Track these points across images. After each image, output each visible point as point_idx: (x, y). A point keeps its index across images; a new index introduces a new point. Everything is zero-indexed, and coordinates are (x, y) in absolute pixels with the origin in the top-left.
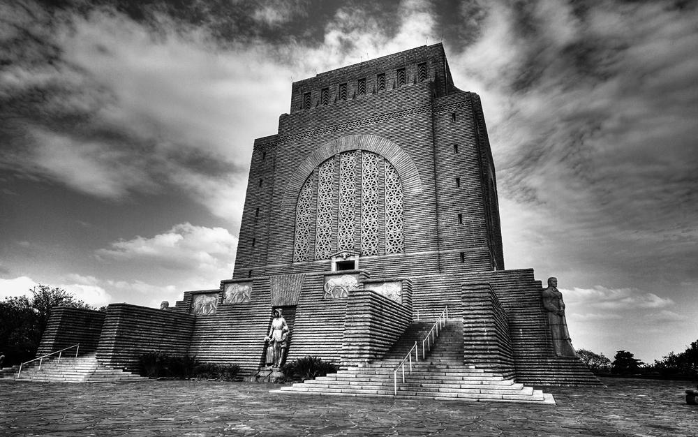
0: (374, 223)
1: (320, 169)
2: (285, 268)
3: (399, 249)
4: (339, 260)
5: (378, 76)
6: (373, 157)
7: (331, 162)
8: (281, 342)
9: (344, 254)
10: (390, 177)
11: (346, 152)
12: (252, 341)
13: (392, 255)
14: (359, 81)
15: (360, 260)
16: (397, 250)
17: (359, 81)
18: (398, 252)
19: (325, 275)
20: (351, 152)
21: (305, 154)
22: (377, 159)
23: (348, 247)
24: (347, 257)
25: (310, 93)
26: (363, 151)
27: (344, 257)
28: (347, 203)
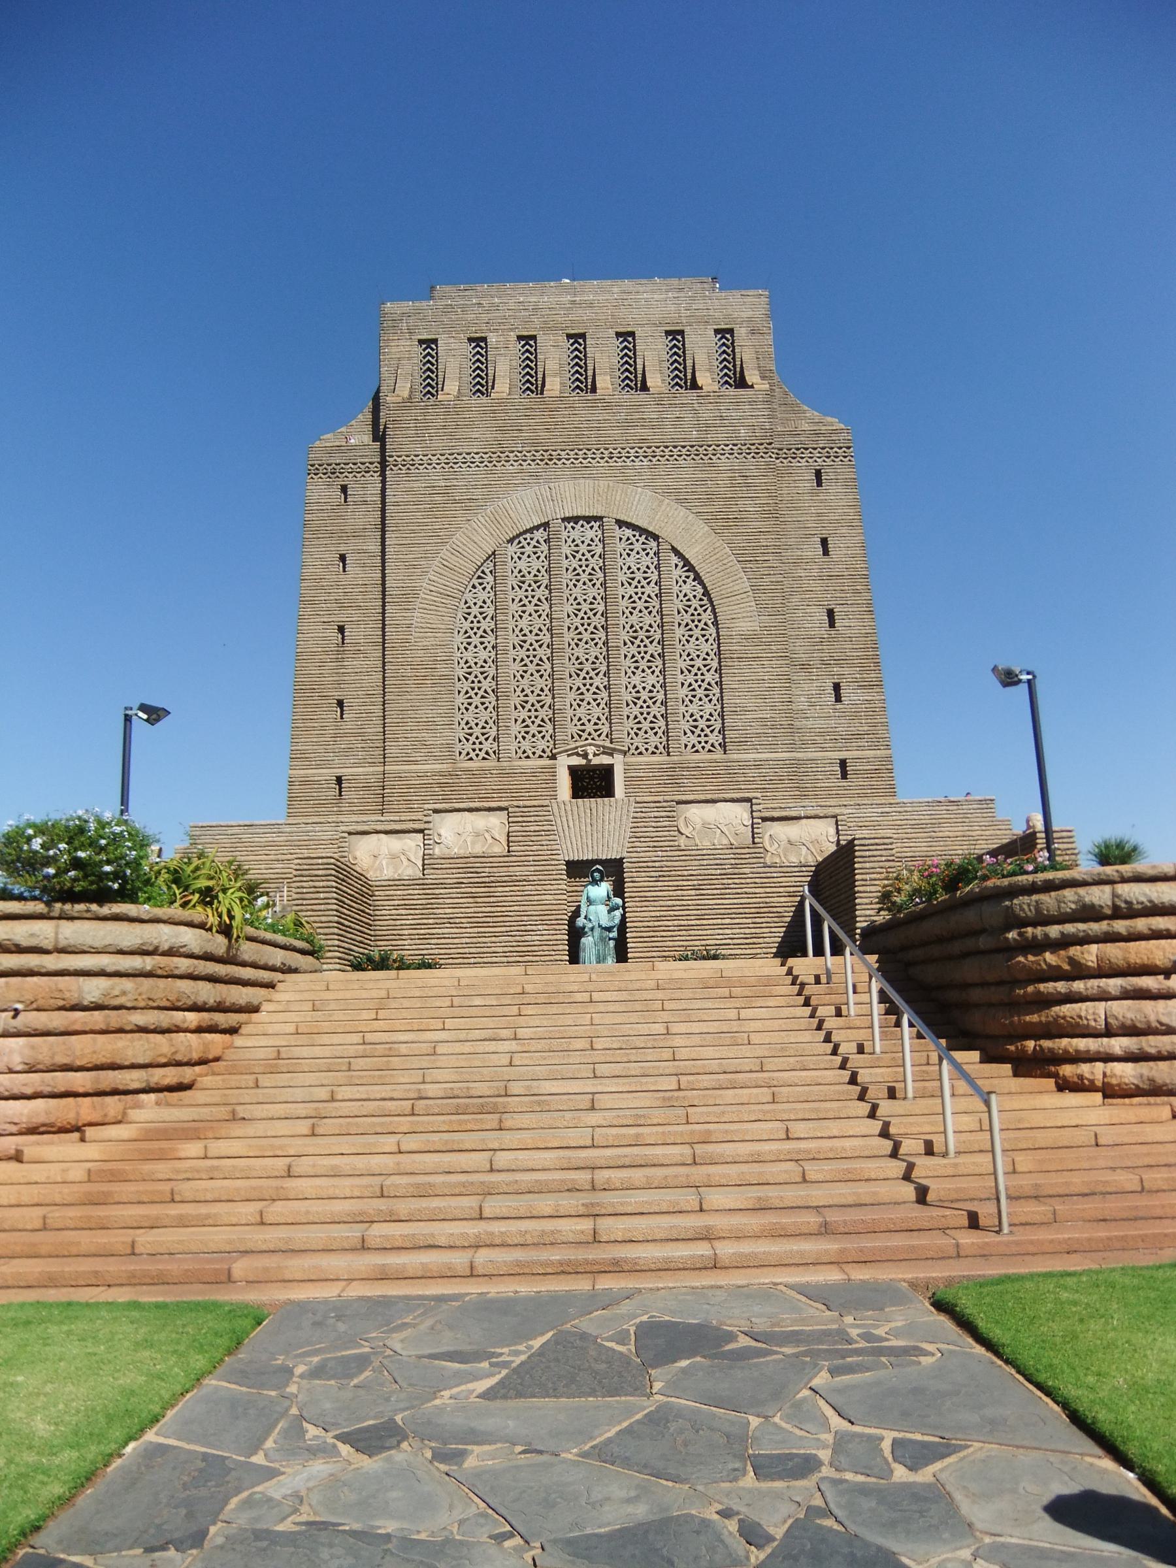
0: (653, 686)
1: (512, 549)
2: (441, 774)
3: (712, 745)
4: (577, 761)
5: (618, 335)
6: (643, 539)
7: (540, 535)
8: (609, 929)
9: (591, 750)
10: (686, 588)
11: (575, 519)
12: (534, 928)
13: (697, 756)
14: (569, 336)
15: (625, 764)
16: (708, 747)
17: (569, 336)
18: (710, 751)
19: (679, 803)
20: (588, 519)
21: (470, 506)
22: (654, 544)
23: (595, 735)
24: (595, 755)
25: (435, 341)
26: (620, 523)
27: (591, 756)
28: (586, 636)
